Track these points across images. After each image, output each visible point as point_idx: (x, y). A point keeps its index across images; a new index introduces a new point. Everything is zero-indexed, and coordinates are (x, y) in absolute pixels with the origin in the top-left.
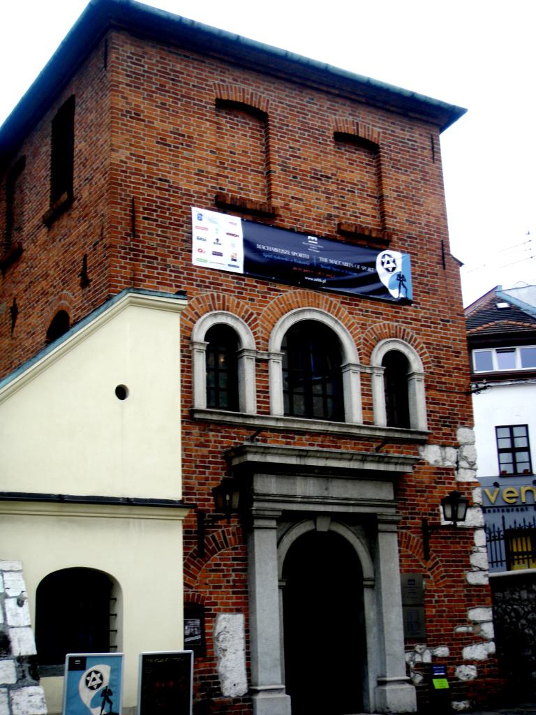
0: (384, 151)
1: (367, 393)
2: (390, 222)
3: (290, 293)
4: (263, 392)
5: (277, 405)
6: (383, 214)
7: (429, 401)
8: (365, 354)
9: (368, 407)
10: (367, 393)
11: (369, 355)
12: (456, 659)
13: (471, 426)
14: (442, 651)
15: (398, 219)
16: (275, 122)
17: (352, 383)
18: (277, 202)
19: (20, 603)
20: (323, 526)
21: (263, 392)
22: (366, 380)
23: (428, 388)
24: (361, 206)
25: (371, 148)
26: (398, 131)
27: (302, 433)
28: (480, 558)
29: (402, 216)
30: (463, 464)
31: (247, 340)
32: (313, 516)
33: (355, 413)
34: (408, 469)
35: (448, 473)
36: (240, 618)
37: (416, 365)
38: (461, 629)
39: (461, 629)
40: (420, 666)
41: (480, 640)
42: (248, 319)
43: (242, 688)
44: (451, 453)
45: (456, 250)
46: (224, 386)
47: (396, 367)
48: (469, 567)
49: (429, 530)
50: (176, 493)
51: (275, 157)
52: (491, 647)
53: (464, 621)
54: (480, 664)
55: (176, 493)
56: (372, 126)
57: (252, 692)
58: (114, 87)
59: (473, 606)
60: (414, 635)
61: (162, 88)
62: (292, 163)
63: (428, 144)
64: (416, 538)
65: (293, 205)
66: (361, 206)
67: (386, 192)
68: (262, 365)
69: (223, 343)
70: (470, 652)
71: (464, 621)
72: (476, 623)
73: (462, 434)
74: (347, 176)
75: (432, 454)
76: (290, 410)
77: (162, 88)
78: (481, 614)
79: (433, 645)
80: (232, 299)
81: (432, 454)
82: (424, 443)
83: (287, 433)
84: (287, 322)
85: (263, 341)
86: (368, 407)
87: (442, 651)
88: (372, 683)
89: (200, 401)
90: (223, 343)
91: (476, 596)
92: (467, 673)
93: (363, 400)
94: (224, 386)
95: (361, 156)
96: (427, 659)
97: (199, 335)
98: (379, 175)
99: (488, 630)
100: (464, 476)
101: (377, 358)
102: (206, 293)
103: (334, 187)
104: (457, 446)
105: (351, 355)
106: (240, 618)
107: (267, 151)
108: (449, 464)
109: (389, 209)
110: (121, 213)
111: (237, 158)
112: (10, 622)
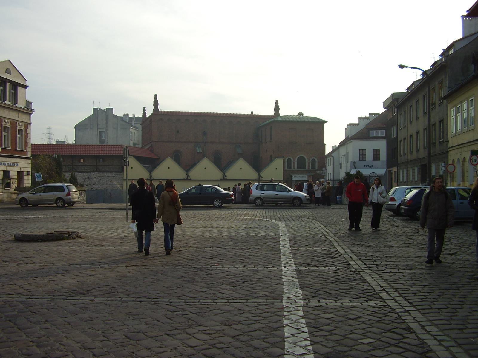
5: (296, 168)
8: (309, 160)
9: (309, 167)
31: (292, 160)
35: (320, 174)
37: (317, 160)
42: (293, 157)
44: (321, 171)
45: (325, 143)
46: (289, 166)
47: (314, 161)
50: (282, 179)
68: (294, 163)
69: (289, 160)
73: (324, 169)
75: (318, 172)
76: (297, 168)
81: (318, 172)
84: (298, 157)
85: (294, 160)
86: (309, 167)
89: (286, 168)
90: (289, 160)
93: (308, 165)
94: (289, 166)
97: (286, 160)
100: (323, 175)
101: (311, 160)
104: (322, 171)
105: (307, 160)
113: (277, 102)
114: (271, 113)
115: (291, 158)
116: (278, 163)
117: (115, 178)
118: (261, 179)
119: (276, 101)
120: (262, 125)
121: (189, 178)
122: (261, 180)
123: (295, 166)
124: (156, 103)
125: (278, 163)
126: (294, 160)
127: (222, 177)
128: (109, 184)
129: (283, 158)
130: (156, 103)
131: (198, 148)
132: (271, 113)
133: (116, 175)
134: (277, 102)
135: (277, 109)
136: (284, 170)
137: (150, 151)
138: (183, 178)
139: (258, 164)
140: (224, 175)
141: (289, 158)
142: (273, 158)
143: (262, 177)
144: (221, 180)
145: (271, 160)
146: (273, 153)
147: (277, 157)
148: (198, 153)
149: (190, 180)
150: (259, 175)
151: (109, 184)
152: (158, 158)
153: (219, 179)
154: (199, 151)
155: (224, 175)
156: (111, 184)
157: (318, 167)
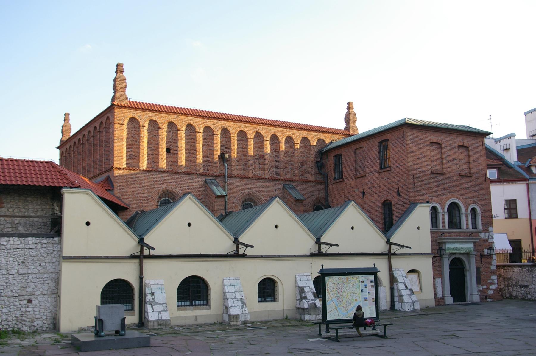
0: (470, 148)
1: (467, 220)
2: (472, 170)
3: (448, 195)
4: (444, 222)
6: (470, 168)
7: (482, 221)
8: (466, 210)
9: (467, 224)
10: (467, 220)
12: (488, 289)
13: (492, 226)
14: (485, 287)
15: (474, 169)
16: (443, 146)
17: (463, 218)
20: (457, 256)
21: (444, 222)
22: (467, 216)
23: (482, 217)
24: (464, 166)
25: (467, 147)
26: (474, 142)
27: (452, 232)
28: (494, 263)
29: (475, 167)
30: (490, 237)
31: (439, 209)
32: (455, 253)
33: (464, 226)
34: (478, 241)
36: (440, 279)
37: (479, 211)
38: (489, 281)
39: (489, 281)
40: (480, 291)
41: (493, 284)
42: (439, 203)
43: (441, 296)
44: (487, 234)
48: (491, 265)
49: (482, 256)
50: (430, 252)
51: (444, 156)
52: (496, 286)
53: (490, 279)
54: (494, 290)
55: (430, 252)
56: (467, 141)
57: (444, 296)
58: (407, 145)
59: (492, 275)
60: (479, 282)
61: (418, 143)
62: (448, 157)
64: (479, 258)
65: (449, 170)
66: (464, 166)
67: (471, 161)
68: (443, 215)
70: (491, 287)
71: (490, 279)
72: (493, 280)
74: (461, 157)
75: (482, 235)
77: (418, 143)
78: (494, 277)
79: (482, 285)
80: (436, 198)
81: (482, 235)
82: (480, 232)
83: (449, 233)
86: (467, 224)
87: (485, 287)
88: (469, 295)
90: (434, 210)
91: (493, 273)
92: (490, 292)
93: (466, 222)
95: (464, 151)
96: (481, 289)
98: (469, 156)
99: (496, 281)
100: (490, 241)
103: (458, 163)
104: (489, 232)
106: (440, 279)
107: (442, 154)
108: (486, 237)
109: (472, 166)
110: (411, 179)
111: (436, 158)
113: (350, 106)
114: (341, 125)
115: (438, 206)
116: (421, 215)
117: (33, 253)
119: (349, 104)
120: (328, 147)
122: (394, 254)
123: (444, 220)
124: (119, 84)
125: (421, 215)
126: (443, 209)
128: (14, 271)
130: (119, 84)
131: (214, 187)
132: (341, 125)
133: (39, 246)
134: (350, 106)
137: (106, 190)
139: (388, 220)
141: (435, 205)
144: (313, 255)
146: (399, 195)
147: (421, 203)
148: (218, 196)
149: (244, 256)
151: (14, 271)
152: (126, 206)
153: (309, 254)
156: (21, 271)
157: (482, 224)
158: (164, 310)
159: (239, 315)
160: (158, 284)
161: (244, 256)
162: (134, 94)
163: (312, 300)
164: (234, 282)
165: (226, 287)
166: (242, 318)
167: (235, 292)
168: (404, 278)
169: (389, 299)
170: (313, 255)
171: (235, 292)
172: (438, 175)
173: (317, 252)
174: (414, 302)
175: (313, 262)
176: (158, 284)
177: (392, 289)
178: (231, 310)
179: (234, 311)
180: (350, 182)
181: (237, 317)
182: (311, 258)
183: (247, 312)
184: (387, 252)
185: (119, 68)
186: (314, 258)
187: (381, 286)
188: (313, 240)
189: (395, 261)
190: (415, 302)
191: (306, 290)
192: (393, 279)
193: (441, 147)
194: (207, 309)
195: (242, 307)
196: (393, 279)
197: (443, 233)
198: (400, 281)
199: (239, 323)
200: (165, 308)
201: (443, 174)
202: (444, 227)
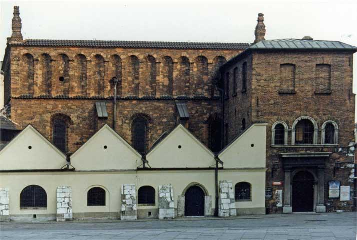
8: (320, 126)
11: (321, 126)
17: (316, 134)
18: (296, 90)
19: (231, 189)
22: (320, 133)
31: (286, 126)
42: (287, 122)
46: (280, 139)
47: (330, 128)
50: (264, 166)
63: (348, 60)
68: (290, 133)
69: (280, 128)
90: (280, 128)
94: (280, 139)
97: (273, 128)
101: (323, 127)
102: (275, 117)
105: (316, 128)
112: (230, 192)
118: (220, 166)
121: (70, 168)
122: (222, 169)
123: (292, 138)
124: (16, 24)
127: (139, 164)
129: (267, 124)
130: (16, 24)
135: (260, 30)
136: (269, 147)
138: (60, 168)
140: (144, 160)
142: (246, 125)
143: (222, 163)
144: (139, 169)
145: (245, 126)
149: (73, 170)
150: (217, 158)
153: (135, 169)
154: (101, 116)
155: (144, 160)
158: (5, 209)
159: (63, 214)
160: (4, 191)
161: (73, 170)
162: (27, 34)
163: (130, 205)
164: (66, 190)
165: (58, 194)
166: (66, 217)
167: (65, 197)
168: (230, 189)
169: (214, 207)
170: (139, 169)
171: (65, 197)
172: (288, 95)
173: (142, 167)
174: (230, 209)
175: (138, 174)
176: (4, 191)
177: (217, 199)
178: (58, 210)
179: (59, 212)
180: (231, 101)
181: (62, 216)
182: (135, 172)
183: (71, 212)
184: (215, 167)
185: (16, 9)
186: (138, 172)
187: (207, 195)
188: (140, 157)
189: (221, 175)
190: (233, 209)
191: (127, 197)
192: (218, 191)
193: (295, 68)
194: (44, 210)
195: (68, 209)
196: (218, 191)
197: (288, 149)
198: (223, 191)
199: (63, 220)
200: (6, 208)
201: (293, 93)
202: (290, 142)
